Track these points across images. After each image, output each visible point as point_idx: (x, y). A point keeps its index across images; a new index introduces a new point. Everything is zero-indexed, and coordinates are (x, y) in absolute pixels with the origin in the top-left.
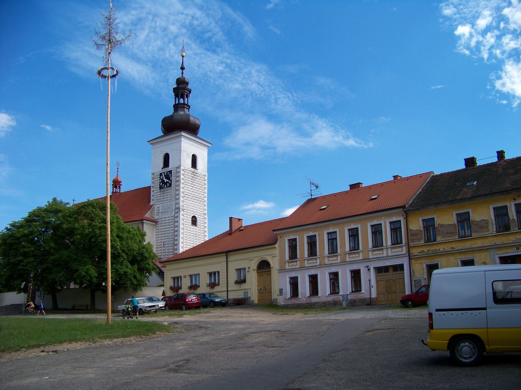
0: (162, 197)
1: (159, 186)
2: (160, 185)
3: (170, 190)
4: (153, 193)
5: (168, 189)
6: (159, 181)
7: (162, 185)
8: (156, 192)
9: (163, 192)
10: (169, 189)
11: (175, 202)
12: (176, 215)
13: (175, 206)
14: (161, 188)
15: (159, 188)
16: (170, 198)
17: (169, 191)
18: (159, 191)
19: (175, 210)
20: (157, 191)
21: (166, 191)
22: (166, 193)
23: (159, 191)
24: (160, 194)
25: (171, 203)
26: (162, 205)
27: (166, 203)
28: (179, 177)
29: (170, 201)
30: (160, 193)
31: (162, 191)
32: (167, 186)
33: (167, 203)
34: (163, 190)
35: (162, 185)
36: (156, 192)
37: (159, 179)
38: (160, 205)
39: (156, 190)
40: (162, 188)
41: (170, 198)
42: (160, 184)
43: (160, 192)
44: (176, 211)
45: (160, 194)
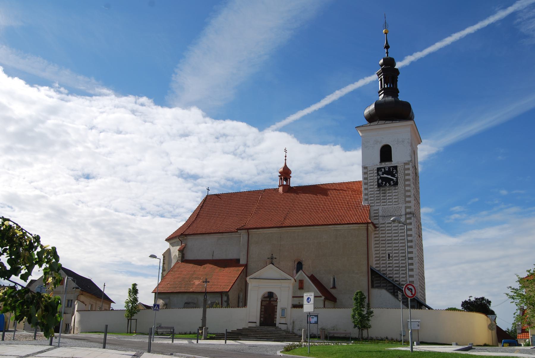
0: (382, 198)
1: (377, 183)
2: (378, 183)
3: (395, 189)
4: (367, 191)
5: (391, 188)
6: (376, 177)
7: (382, 183)
8: (371, 190)
9: (384, 192)
10: (393, 188)
11: (404, 205)
12: (408, 221)
13: (406, 210)
14: (379, 185)
15: (377, 186)
16: (397, 200)
17: (394, 191)
18: (377, 189)
19: (406, 214)
20: (373, 189)
21: (389, 190)
22: (389, 193)
23: (377, 189)
24: (379, 194)
25: (398, 206)
26: (383, 208)
27: (395, 205)
28: (364, 178)
29: (397, 203)
30: (378, 192)
31: (382, 190)
32: (390, 184)
33: (391, 205)
34: (383, 189)
35: (382, 183)
36: (371, 190)
37: (376, 174)
38: (380, 208)
39: (370, 188)
40: (383, 186)
41: (397, 200)
42: (378, 181)
43: (378, 191)
44: (408, 216)
45: (379, 194)
